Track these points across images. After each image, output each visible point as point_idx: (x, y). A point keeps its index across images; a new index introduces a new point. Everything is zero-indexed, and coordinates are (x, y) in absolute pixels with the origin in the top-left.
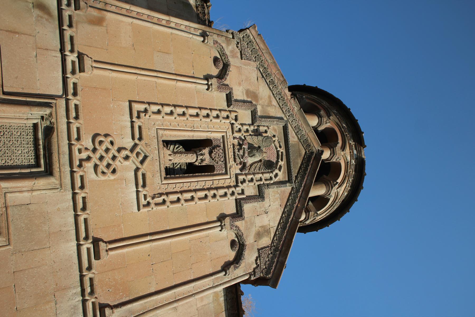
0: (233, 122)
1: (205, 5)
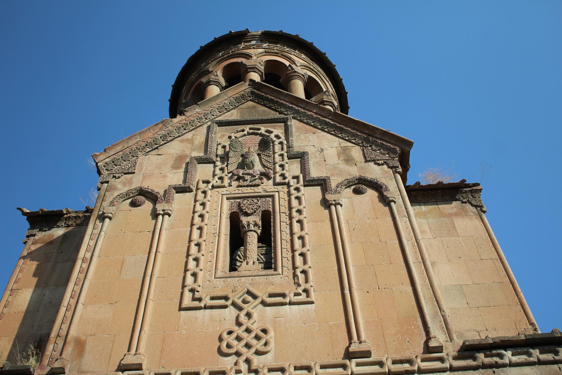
0: (210, 186)
1: (66, 216)
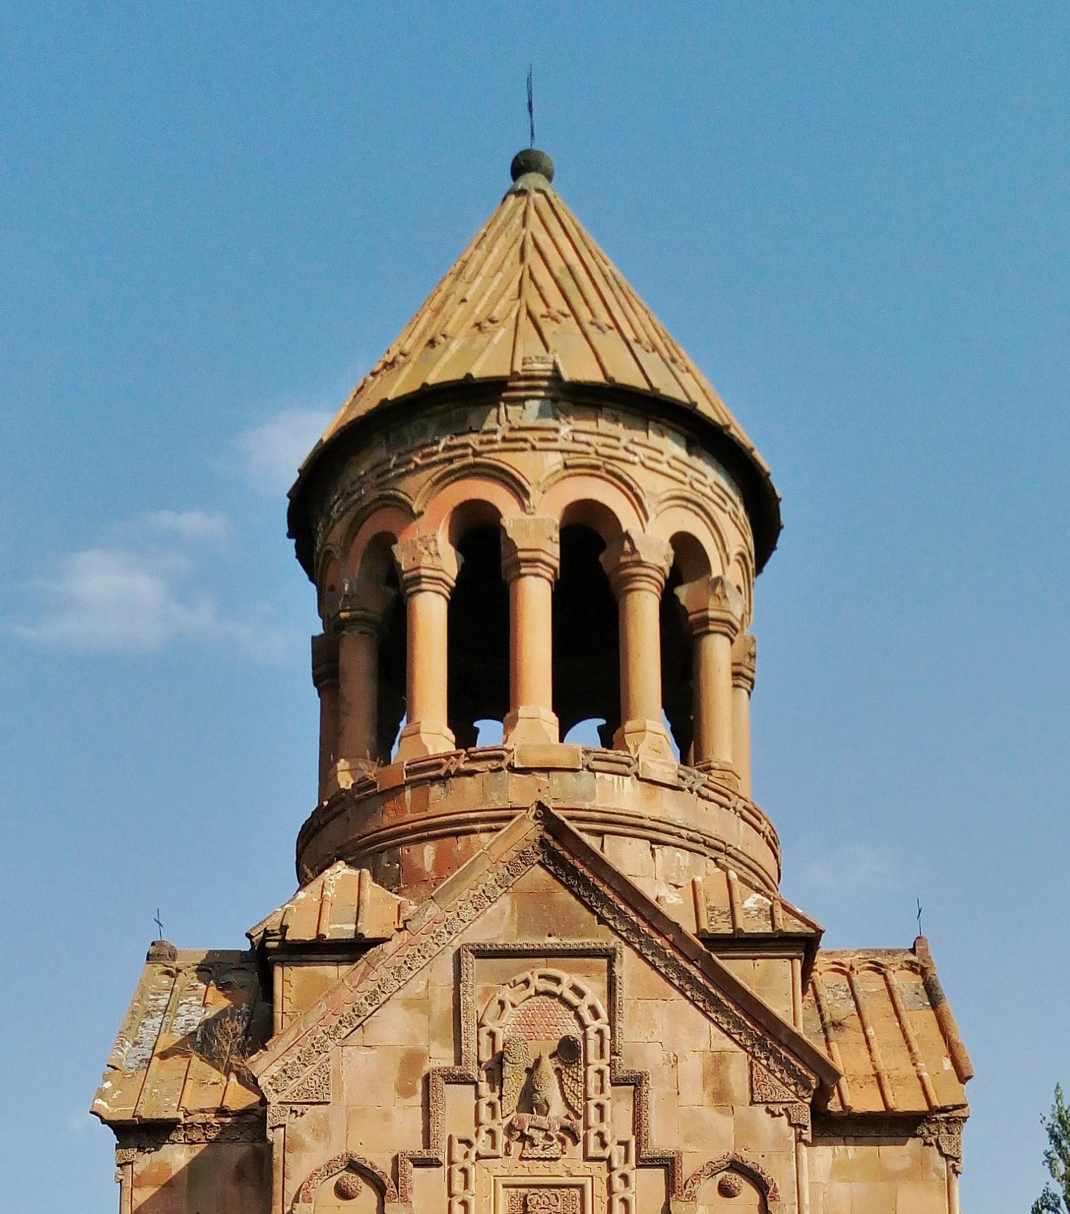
1: (184, 1121)
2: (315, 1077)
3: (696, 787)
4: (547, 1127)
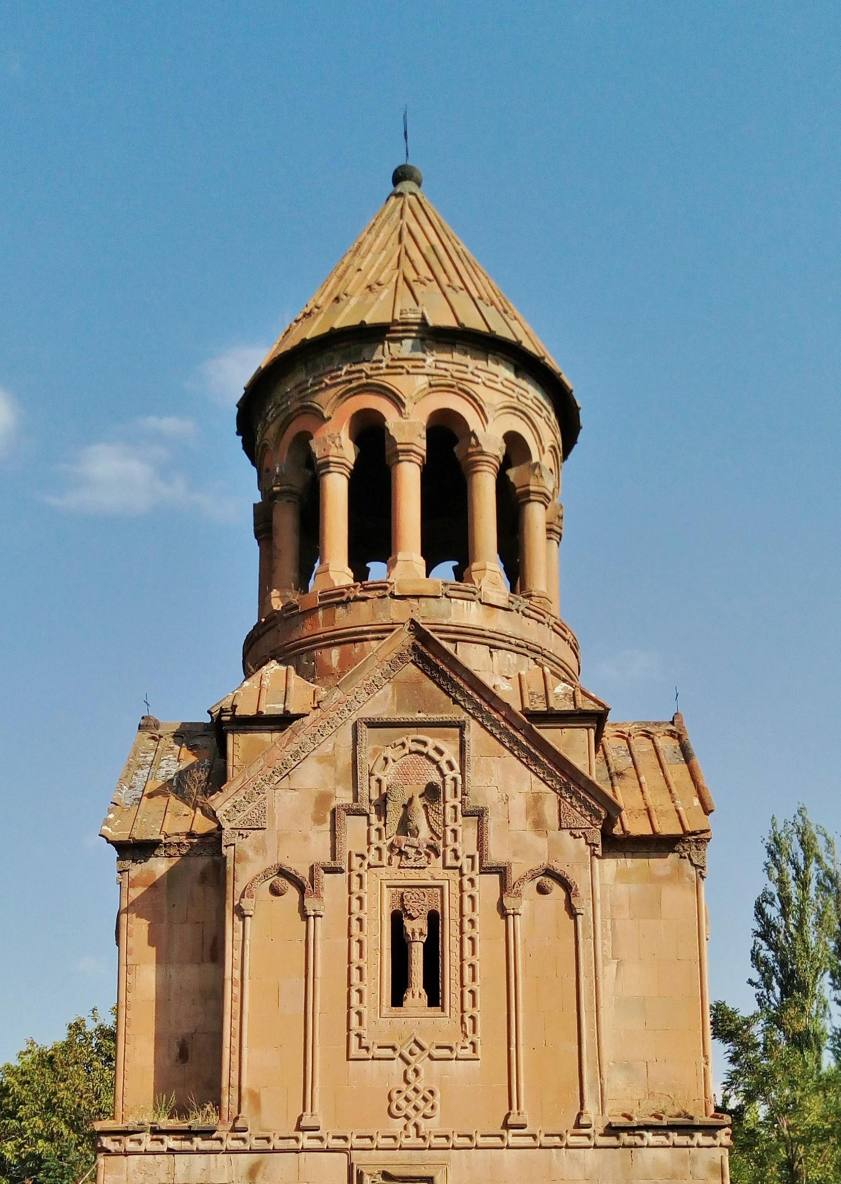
1: (164, 841)
2: (256, 811)
3: (521, 609)
4: (417, 845)
